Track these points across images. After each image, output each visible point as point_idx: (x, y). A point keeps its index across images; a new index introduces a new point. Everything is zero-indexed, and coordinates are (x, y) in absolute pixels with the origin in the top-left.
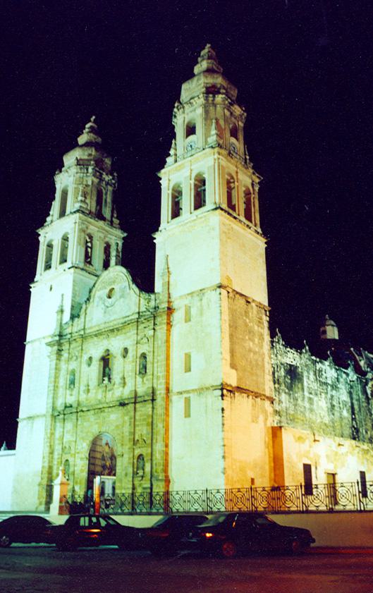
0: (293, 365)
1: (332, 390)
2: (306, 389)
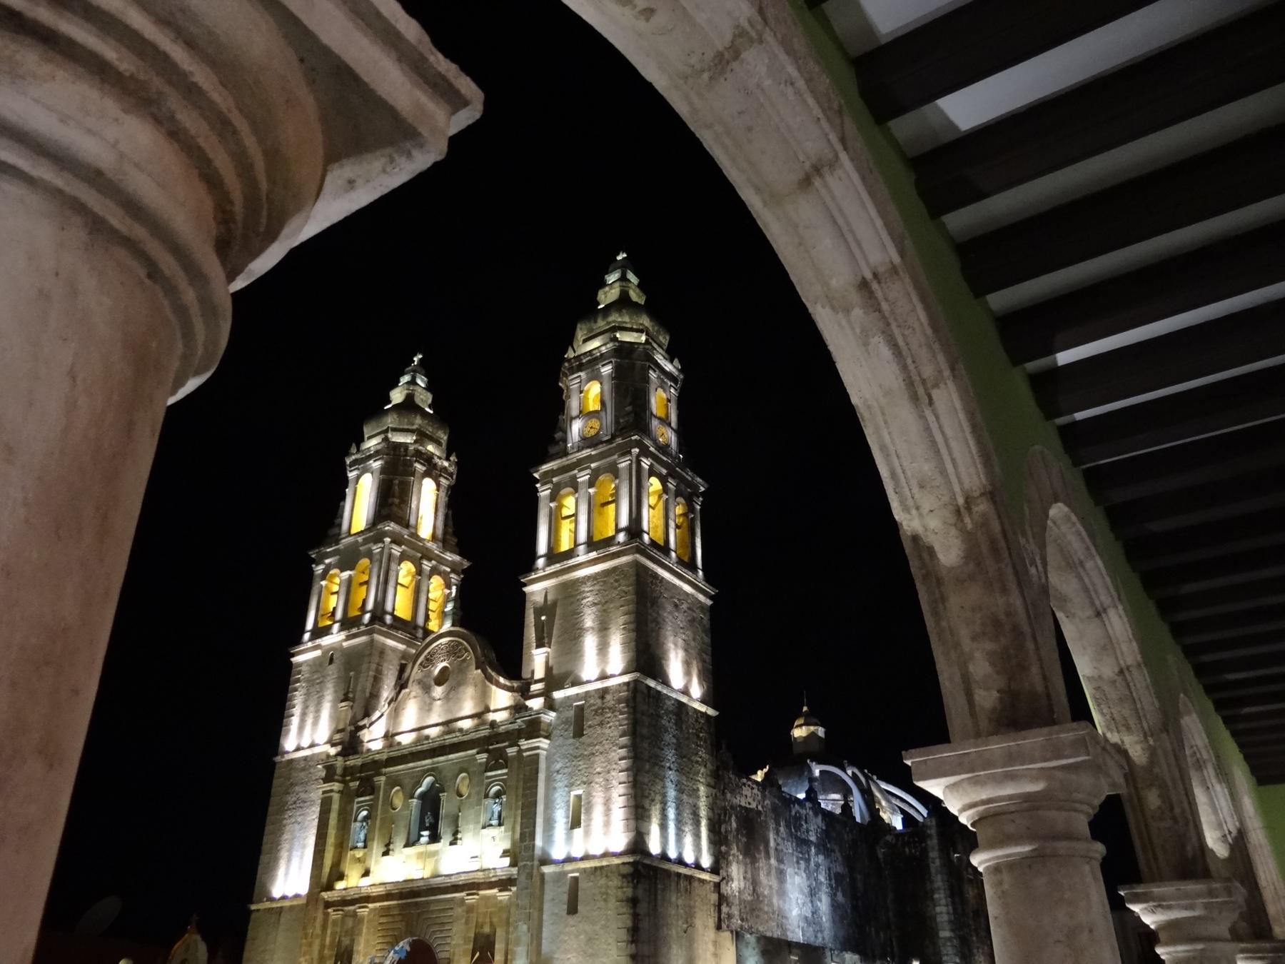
0: (751, 810)
1: (817, 854)
2: (772, 852)
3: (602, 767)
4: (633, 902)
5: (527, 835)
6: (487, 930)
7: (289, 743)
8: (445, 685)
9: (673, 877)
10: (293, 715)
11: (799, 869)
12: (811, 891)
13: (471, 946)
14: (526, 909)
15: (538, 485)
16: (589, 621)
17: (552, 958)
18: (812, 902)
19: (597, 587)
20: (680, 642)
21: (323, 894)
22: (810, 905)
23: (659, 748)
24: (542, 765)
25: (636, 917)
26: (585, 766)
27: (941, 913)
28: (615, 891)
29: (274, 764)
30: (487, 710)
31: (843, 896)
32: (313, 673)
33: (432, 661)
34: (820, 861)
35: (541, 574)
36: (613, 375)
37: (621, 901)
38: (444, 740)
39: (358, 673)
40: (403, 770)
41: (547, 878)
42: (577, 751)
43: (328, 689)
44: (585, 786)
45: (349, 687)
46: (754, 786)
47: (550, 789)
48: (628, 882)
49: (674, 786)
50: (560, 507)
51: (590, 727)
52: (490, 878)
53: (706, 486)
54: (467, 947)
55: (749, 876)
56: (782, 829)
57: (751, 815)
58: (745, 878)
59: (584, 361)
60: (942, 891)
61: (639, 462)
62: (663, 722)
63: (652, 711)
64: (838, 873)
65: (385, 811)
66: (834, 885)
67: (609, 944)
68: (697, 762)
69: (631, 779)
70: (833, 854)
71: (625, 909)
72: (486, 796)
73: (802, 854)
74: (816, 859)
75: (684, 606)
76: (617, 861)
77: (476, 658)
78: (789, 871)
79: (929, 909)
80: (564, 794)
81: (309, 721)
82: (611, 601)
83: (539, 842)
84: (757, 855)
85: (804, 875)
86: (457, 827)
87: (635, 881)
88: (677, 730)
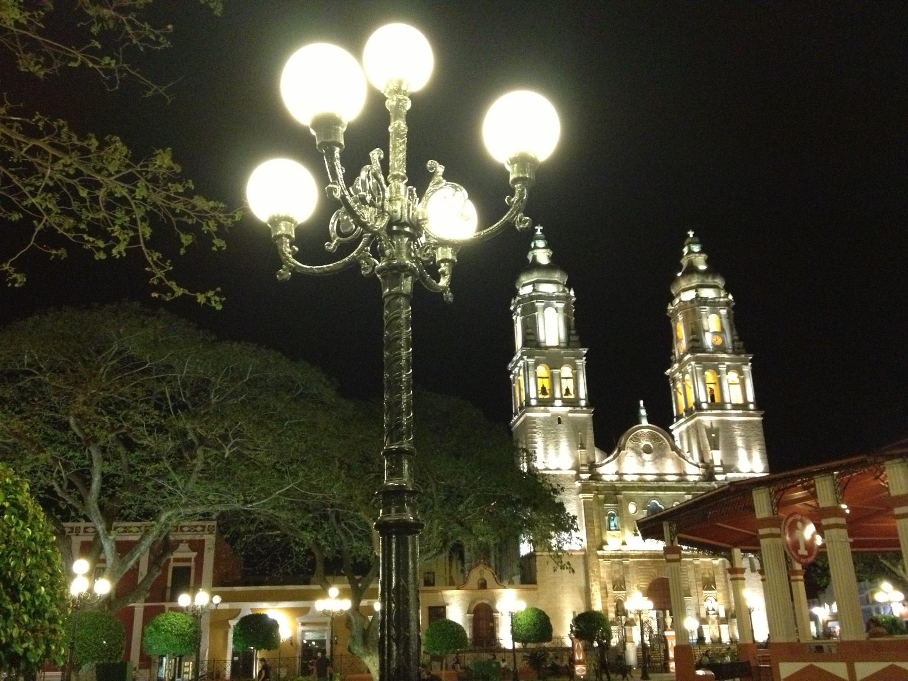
6: (707, 576)
16: (740, 442)
82: (751, 436)
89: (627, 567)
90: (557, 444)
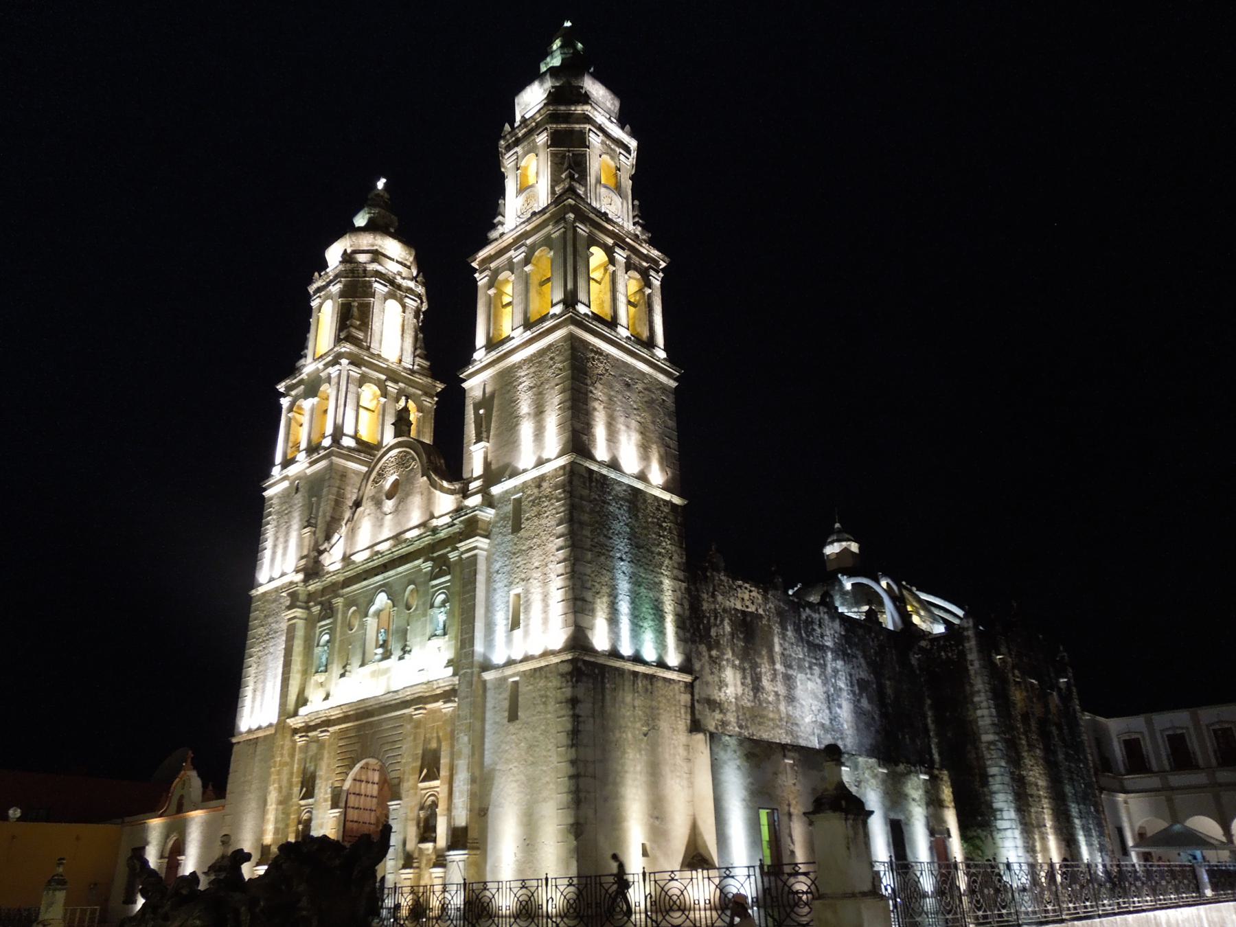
1: (834, 660)
2: (778, 658)
3: (540, 561)
4: (573, 702)
5: (467, 641)
6: (434, 745)
7: (263, 576)
8: (395, 498)
9: (626, 675)
10: (266, 549)
11: (812, 674)
12: (828, 696)
13: (419, 763)
14: (466, 719)
15: (476, 275)
16: (525, 406)
17: (494, 770)
18: (829, 708)
19: (532, 370)
20: (634, 424)
21: (288, 721)
22: (827, 711)
23: (605, 536)
24: (482, 566)
25: (576, 718)
26: (524, 562)
27: (983, 716)
28: (554, 692)
29: (250, 599)
30: (432, 517)
31: (869, 703)
32: (282, 504)
33: (383, 475)
34: (839, 667)
35: (478, 366)
36: (549, 143)
37: (561, 703)
38: (392, 553)
39: (319, 497)
40: (358, 590)
41: (489, 685)
42: (515, 547)
43: (294, 518)
44: (523, 583)
45: (311, 513)
46: (753, 589)
47: (490, 591)
48: (568, 682)
49: (627, 578)
50: (500, 294)
51: (527, 519)
52: (434, 690)
53: (667, 260)
54: (414, 765)
55: (749, 681)
56: (789, 633)
57: (749, 619)
58: (743, 684)
59: (520, 135)
60: (982, 694)
61: (575, 228)
62: (611, 509)
63: (594, 496)
64: (862, 679)
65: (343, 633)
66: (857, 692)
67: (549, 750)
68: (660, 554)
69: (568, 570)
70: (854, 660)
71: (566, 711)
72: (432, 606)
73: (816, 659)
74: (834, 665)
75: (640, 386)
76: (554, 660)
77: (422, 465)
78: (800, 677)
79: (969, 713)
80: (503, 594)
81: (280, 551)
83: (479, 648)
84: (758, 660)
85: (819, 681)
86: (406, 641)
87: (574, 679)
88: (630, 518)
89: (321, 744)
90: (287, 534)
